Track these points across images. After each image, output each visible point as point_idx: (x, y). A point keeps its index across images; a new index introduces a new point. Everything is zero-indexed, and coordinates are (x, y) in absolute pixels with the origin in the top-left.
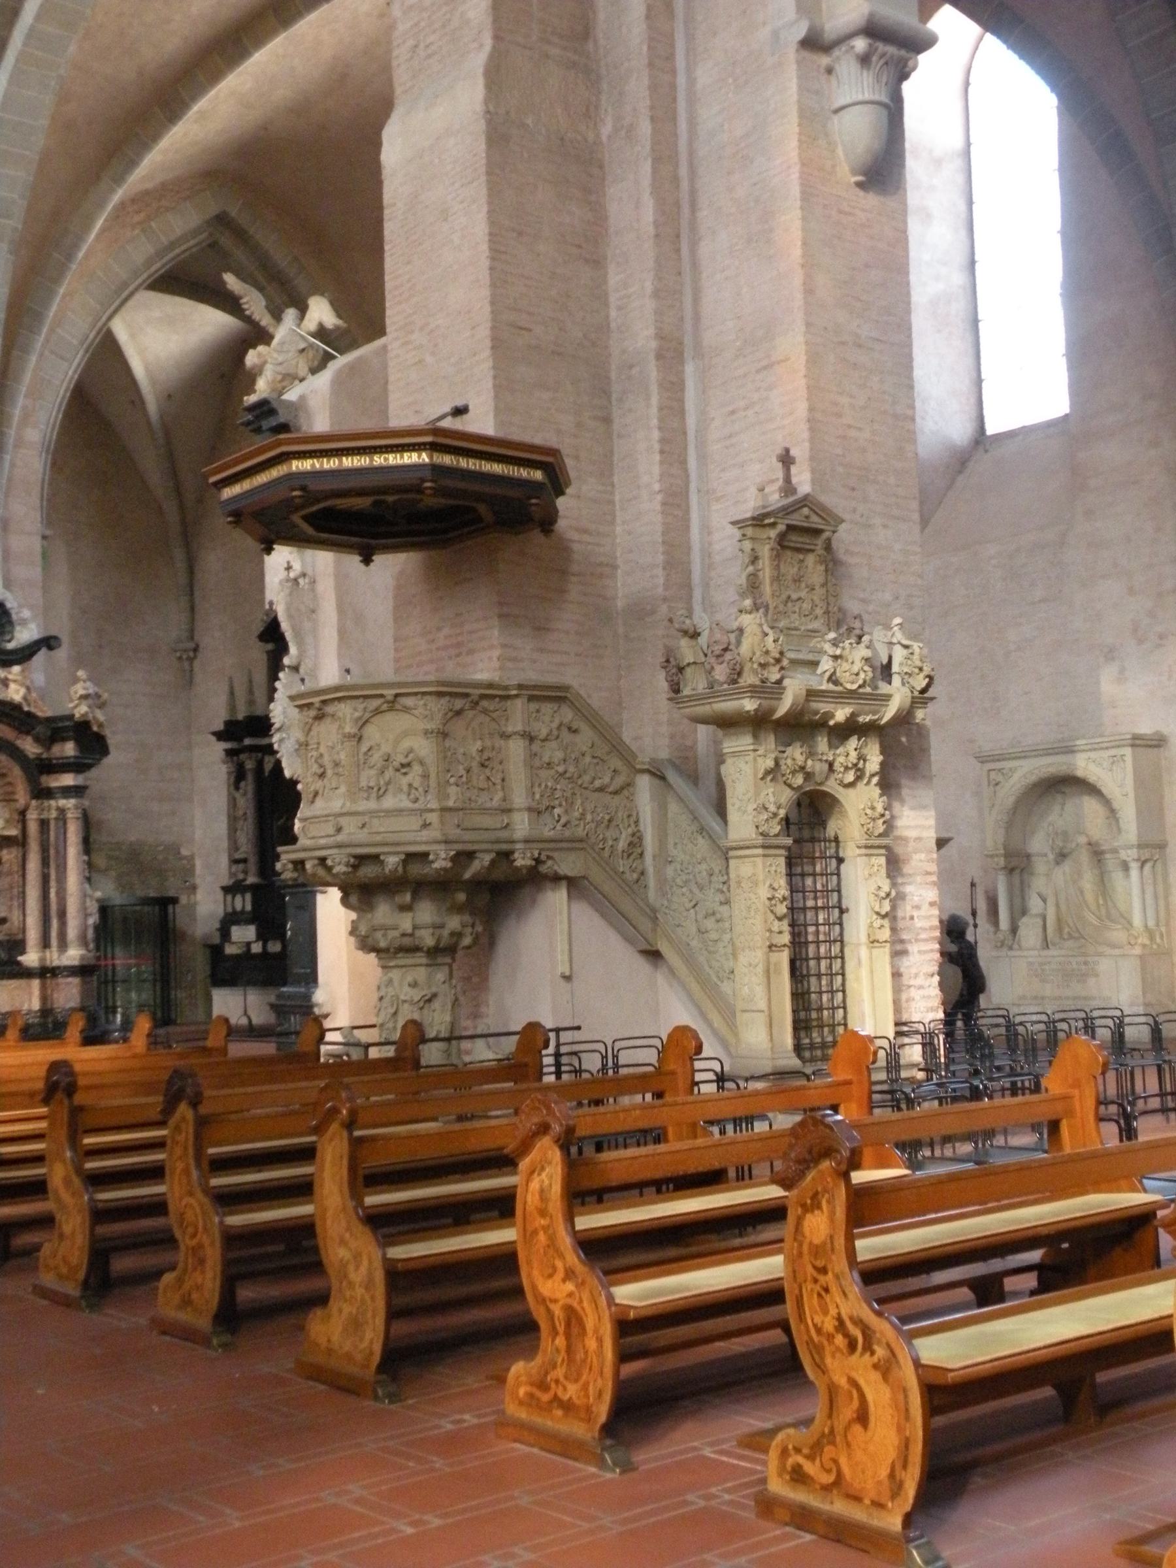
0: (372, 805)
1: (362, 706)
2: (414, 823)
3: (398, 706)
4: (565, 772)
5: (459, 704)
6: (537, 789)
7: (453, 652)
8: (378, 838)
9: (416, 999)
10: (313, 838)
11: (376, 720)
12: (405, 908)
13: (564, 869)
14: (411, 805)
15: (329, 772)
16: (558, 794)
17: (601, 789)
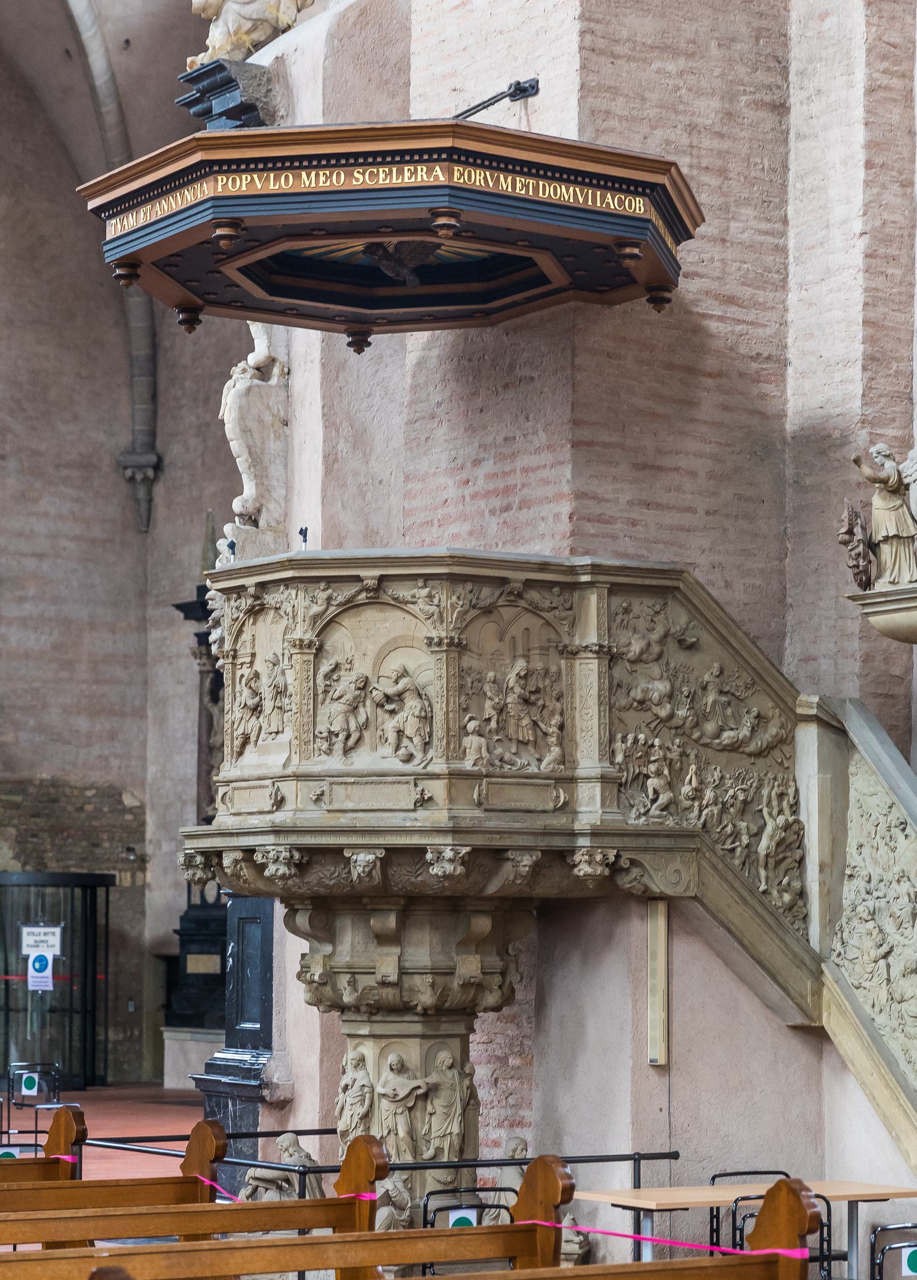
0: (335, 763)
1: (324, 595)
2: (406, 796)
3: (385, 598)
4: (671, 716)
5: (487, 594)
6: (618, 746)
7: (497, 503)
8: (344, 820)
9: (402, 1094)
10: (238, 814)
11: (347, 621)
12: (383, 939)
13: (659, 883)
14: (398, 766)
15: (268, 705)
16: (657, 754)
17: (734, 747)
